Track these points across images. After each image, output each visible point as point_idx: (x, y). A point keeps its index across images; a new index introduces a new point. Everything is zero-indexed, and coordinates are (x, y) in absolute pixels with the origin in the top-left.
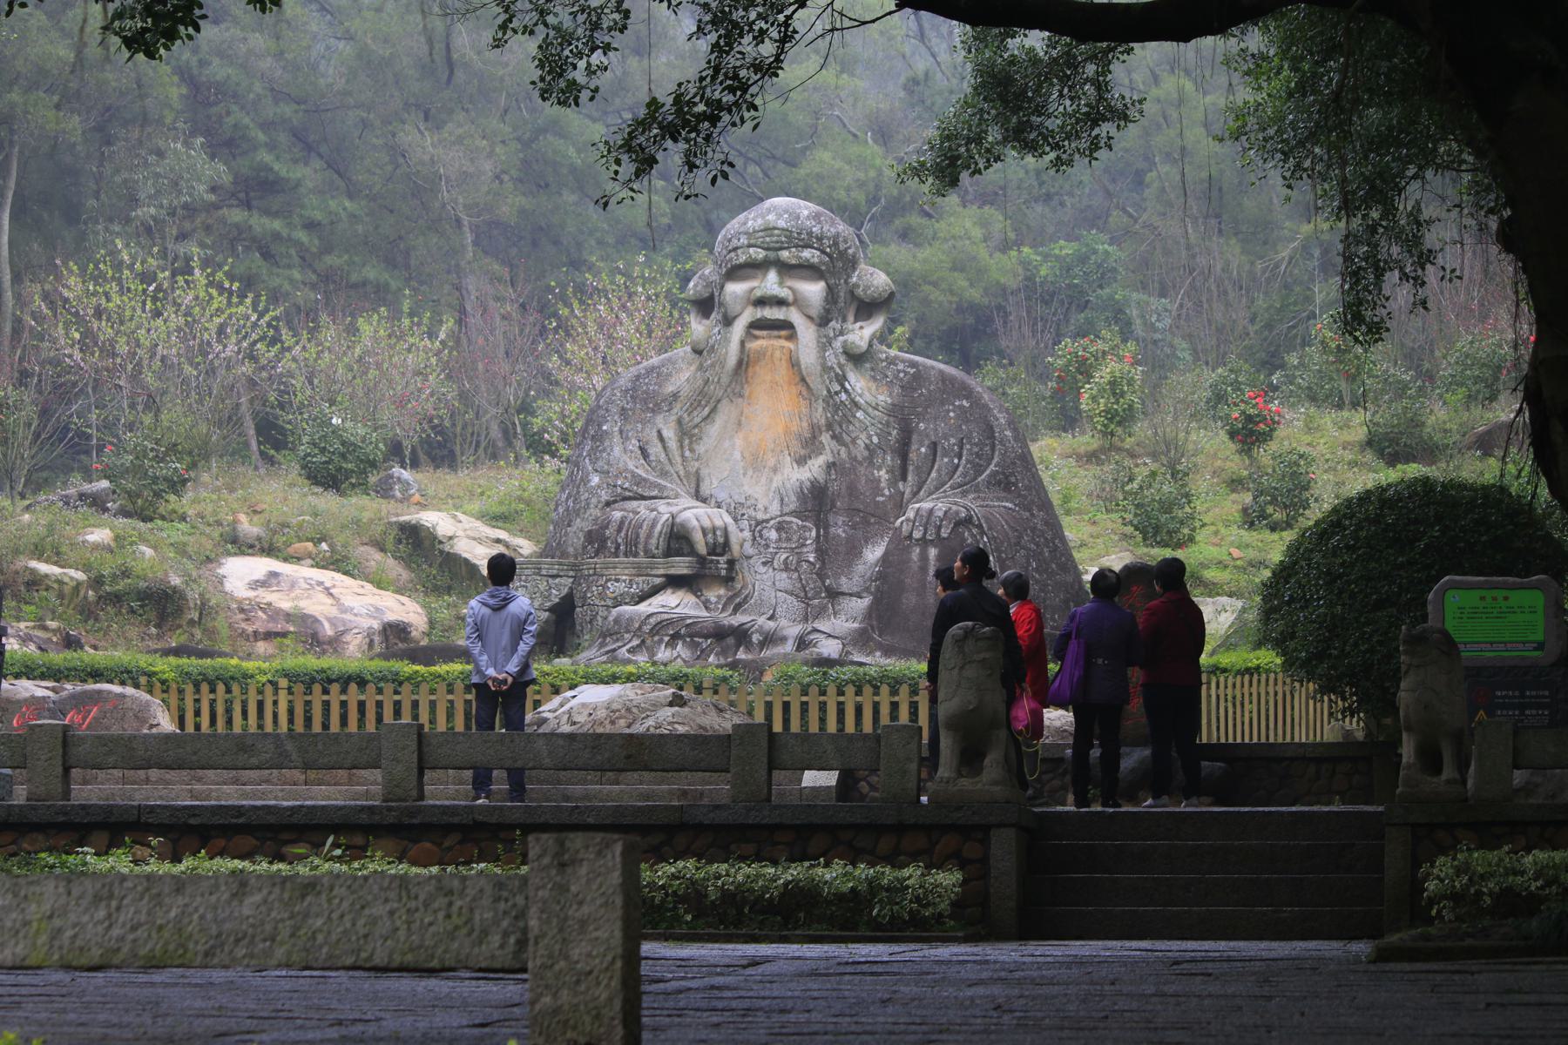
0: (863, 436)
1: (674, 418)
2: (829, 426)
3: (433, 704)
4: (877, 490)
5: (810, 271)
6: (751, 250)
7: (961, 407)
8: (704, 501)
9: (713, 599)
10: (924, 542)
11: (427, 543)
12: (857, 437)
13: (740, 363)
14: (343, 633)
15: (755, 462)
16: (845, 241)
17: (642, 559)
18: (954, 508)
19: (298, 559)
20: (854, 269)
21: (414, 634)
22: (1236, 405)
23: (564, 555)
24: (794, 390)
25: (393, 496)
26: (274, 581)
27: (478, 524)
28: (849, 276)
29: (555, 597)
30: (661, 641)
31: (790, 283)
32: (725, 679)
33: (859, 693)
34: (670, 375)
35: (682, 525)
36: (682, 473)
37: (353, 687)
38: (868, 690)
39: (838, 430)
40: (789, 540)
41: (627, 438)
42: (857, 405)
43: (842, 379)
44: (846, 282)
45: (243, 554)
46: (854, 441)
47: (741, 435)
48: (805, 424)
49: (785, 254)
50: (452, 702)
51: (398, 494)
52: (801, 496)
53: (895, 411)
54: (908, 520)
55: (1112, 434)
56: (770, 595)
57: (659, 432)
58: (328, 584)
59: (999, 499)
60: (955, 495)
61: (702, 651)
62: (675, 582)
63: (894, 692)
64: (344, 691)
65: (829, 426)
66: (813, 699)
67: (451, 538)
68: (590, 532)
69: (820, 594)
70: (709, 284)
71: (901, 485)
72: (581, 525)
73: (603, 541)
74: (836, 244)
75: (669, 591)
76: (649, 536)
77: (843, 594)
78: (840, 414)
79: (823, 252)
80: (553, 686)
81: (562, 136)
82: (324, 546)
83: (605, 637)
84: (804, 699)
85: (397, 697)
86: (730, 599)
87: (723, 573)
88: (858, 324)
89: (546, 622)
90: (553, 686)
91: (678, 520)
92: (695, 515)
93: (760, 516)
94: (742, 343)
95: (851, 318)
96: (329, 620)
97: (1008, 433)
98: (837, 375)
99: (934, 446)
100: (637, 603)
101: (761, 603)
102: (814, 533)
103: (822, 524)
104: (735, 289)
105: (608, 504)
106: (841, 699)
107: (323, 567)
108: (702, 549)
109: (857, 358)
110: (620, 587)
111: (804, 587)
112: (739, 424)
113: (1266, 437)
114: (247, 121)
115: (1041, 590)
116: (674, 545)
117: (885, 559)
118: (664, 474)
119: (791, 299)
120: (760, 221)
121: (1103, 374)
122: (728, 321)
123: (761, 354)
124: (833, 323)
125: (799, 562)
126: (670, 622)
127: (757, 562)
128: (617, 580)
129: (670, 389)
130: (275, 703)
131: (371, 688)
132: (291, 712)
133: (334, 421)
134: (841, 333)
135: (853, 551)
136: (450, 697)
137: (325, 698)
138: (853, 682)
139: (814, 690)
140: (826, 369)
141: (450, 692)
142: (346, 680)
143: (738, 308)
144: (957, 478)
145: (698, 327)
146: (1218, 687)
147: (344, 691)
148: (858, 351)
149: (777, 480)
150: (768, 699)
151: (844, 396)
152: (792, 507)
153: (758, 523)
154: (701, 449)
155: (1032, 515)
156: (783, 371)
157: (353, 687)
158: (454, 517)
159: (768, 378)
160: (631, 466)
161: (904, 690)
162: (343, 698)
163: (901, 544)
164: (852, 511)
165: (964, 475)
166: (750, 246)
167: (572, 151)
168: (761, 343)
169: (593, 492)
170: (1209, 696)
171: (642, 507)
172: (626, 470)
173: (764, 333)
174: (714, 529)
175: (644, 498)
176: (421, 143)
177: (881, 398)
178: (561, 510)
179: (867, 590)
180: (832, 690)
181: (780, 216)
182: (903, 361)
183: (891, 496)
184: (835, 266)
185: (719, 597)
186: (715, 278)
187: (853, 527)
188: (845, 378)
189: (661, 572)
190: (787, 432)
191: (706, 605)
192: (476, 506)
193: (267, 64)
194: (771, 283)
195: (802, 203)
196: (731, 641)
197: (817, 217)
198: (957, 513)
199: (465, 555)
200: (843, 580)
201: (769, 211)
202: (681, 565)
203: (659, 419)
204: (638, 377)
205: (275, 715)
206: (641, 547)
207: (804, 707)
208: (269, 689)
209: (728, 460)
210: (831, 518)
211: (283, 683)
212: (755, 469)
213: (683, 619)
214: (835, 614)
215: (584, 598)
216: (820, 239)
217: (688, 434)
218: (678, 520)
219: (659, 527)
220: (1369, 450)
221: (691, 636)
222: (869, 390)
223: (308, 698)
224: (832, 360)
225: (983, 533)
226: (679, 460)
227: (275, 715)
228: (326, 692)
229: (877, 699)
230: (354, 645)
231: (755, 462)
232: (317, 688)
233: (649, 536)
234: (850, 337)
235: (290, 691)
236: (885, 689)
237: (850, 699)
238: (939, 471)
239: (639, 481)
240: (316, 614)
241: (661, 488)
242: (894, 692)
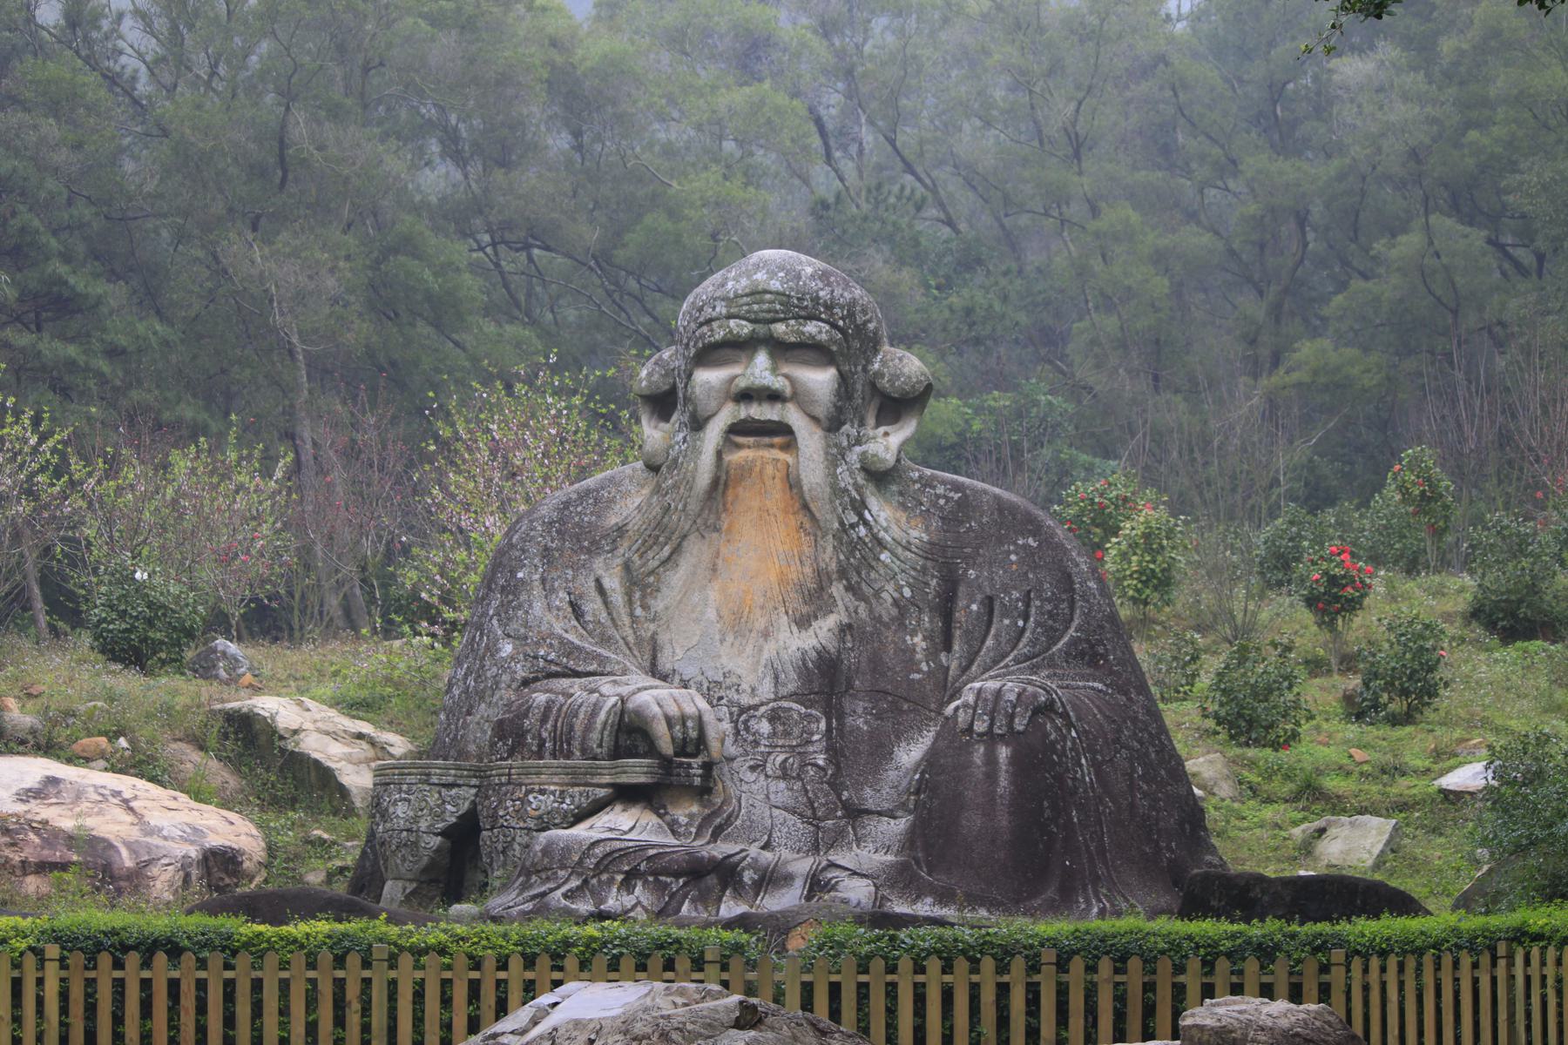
0: (890, 587)
1: (619, 561)
2: (843, 573)
3: (284, 985)
4: (912, 665)
6: (732, 323)
7: (1026, 547)
8: (664, 678)
9: (683, 820)
10: (990, 738)
11: (263, 739)
12: (882, 589)
13: (715, 483)
14: (148, 863)
15: (737, 624)
16: (864, 312)
17: (577, 761)
18: (1030, 688)
19: (85, 760)
20: (876, 351)
21: (246, 864)
22: (1313, 563)
23: (462, 754)
24: (793, 521)
25: (217, 677)
26: (52, 790)
27: (332, 713)
28: (869, 362)
29: (451, 815)
30: (611, 881)
31: (786, 369)
32: (738, 948)
33: (947, 968)
34: (612, 501)
35: (638, 713)
36: (631, 639)
37: (161, 958)
38: (961, 965)
39: (855, 579)
40: (787, 734)
41: (553, 590)
42: (881, 543)
43: (859, 507)
44: (865, 370)
45: (11, 752)
46: (877, 594)
47: (716, 585)
48: (808, 570)
49: (780, 328)
50: (313, 982)
51: (223, 673)
52: (803, 670)
53: (932, 551)
54: (966, 706)
55: (1146, 603)
56: (762, 811)
57: (598, 581)
58: (127, 795)
59: (1083, 678)
60: (1021, 671)
61: (672, 896)
62: (626, 795)
63: (1002, 968)
64: (146, 964)
65: (843, 573)
66: (876, 979)
67: (295, 732)
68: (501, 722)
69: (835, 814)
70: (669, 373)
71: (943, 657)
72: (487, 712)
73: (520, 735)
74: (851, 315)
75: (618, 808)
76: (588, 728)
77: (869, 812)
78: (857, 557)
79: (834, 326)
80: (471, 957)
81: (419, 258)
82: (123, 742)
83: (528, 874)
84: (863, 978)
85: (229, 974)
86: (707, 820)
87: (697, 781)
88: (882, 429)
89: (438, 850)
90: (471, 957)
91: (630, 705)
92: (653, 698)
93: (746, 700)
94: (719, 454)
95: (871, 421)
96: (128, 845)
97: (1091, 584)
98: (853, 500)
99: (989, 603)
100: (572, 825)
101: (751, 825)
102: (823, 726)
103: (833, 711)
104: (709, 378)
105: (526, 682)
106: (920, 978)
107: (121, 772)
108: (666, 747)
109: (880, 477)
110: (548, 802)
111: (811, 803)
112: (714, 569)
113: (1353, 605)
114: (36, 223)
115: (1152, 808)
116: (625, 741)
117: (931, 760)
118: (605, 640)
119: (788, 391)
120: (744, 282)
121: (1130, 528)
122: (698, 424)
123: (746, 470)
124: (846, 427)
125: (803, 766)
126: (624, 854)
127: (742, 766)
128: (542, 792)
129: (613, 520)
130: (40, 982)
131: (188, 959)
132: (64, 996)
133: (138, 575)
134: (858, 442)
135: (881, 751)
136: (311, 974)
137: (118, 974)
138: (938, 952)
139: (878, 965)
141: (312, 965)
142: (149, 947)
143: (713, 404)
144: (1023, 647)
145: (653, 433)
146: (1527, 962)
147: (146, 964)
148: (882, 467)
149: (769, 650)
150: (807, 978)
151: (862, 531)
152: (791, 687)
153: (743, 710)
154: (658, 605)
155: (1130, 699)
156: (776, 495)
157: (161, 958)
158: (300, 704)
159: (756, 504)
160: (558, 630)
161: (1018, 964)
162: (146, 974)
163: (955, 740)
164: (876, 694)
165: (1033, 643)
166: (730, 317)
167: (427, 274)
168: (746, 453)
169: (503, 666)
170: (1511, 978)
171: (576, 687)
172: (551, 635)
173: (751, 440)
174: (684, 719)
175: (578, 674)
176: (250, 257)
177: (914, 533)
178: (456, 692)
179: (903, 806)
180: (905, 964)
181: (772, 275)
182: (943, 482)
183: (929, 672)
184: (849, 346)
185: (691, 816)
186: (679, 363)
187: (878, 717)
188: (864, 505)
189: (607, 779)
190: (782, 581)
191: (673, 828)
192: (328, 689)
193: (61, 157)
195: (803, 257)
196: (712, 880)
197: (824, 276)
198: (1035, 696)
199: (315, 755)
200: (868, 791)
201: (757, 267)
202: (637, 771)
203: (598, 564)
204: (567, 504)
205: (40, 1002)
206: (576, 743)
207: (863, 991)
208: (30, 961)
209: (697, 621)
210: (847, 704)
211: (53, 951)
212: (737, 634)
213: (643, 848)
214: (858, 841)
215: (495, 817)
216: (829, 307)
217: (639, 584)
218: (630, 705)
219: (602, 716)
220: (1474, 624)
221: (656, 873)
222: (898, 521)
223: (92, 974)
224: (845, 480)
225: (1070, 725)
226: (626, 620)
227: (40, 1002)
228: (118, 964)
229: (975, 978)
230: (162, 881)
231: (737, 624)
232: (105, 960)
233: (588, 728)
234: (872, 448)
235: (63, 963)
236: (988, 964)
237: (934, 978)
238: (997, 636)
239: (571, 650)
240: (111, 837)
241: (602, 660)
242: (1002, 968)
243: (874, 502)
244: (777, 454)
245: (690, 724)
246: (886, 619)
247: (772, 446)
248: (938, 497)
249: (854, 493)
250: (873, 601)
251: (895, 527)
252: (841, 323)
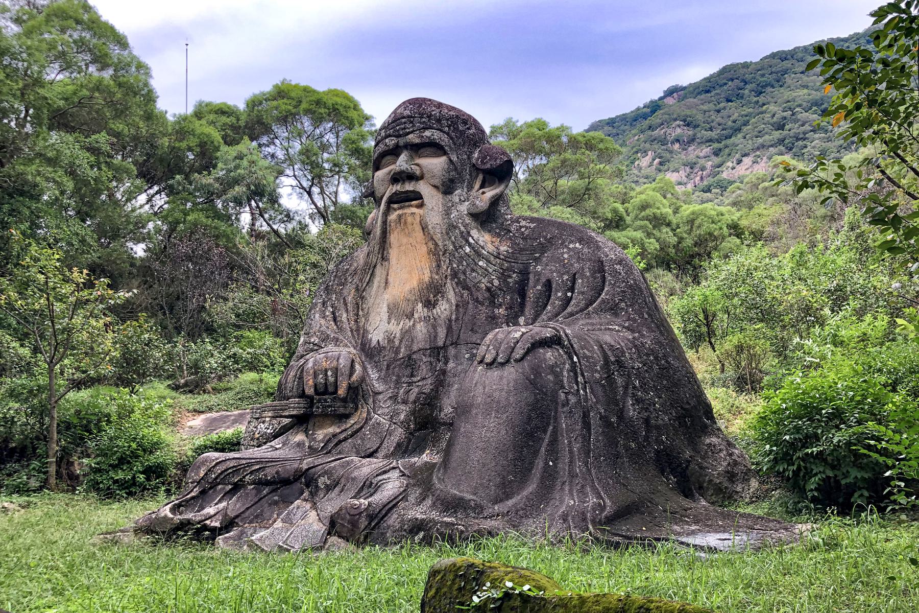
5: (436, 148)
39: (462, 277)
42: (479, 254)
43: (466, 236)
98: (462, 233)
119: (418, 173)
213: (250, 465)
216: (439, 121)
243: (474, 233)
244: (414, 210)
245: (329, 373)
246: (480, 299)
248: (521, 227)
249: (462, 228)
250: (473, 290)
251: (489, 245)
252: (446, 129)
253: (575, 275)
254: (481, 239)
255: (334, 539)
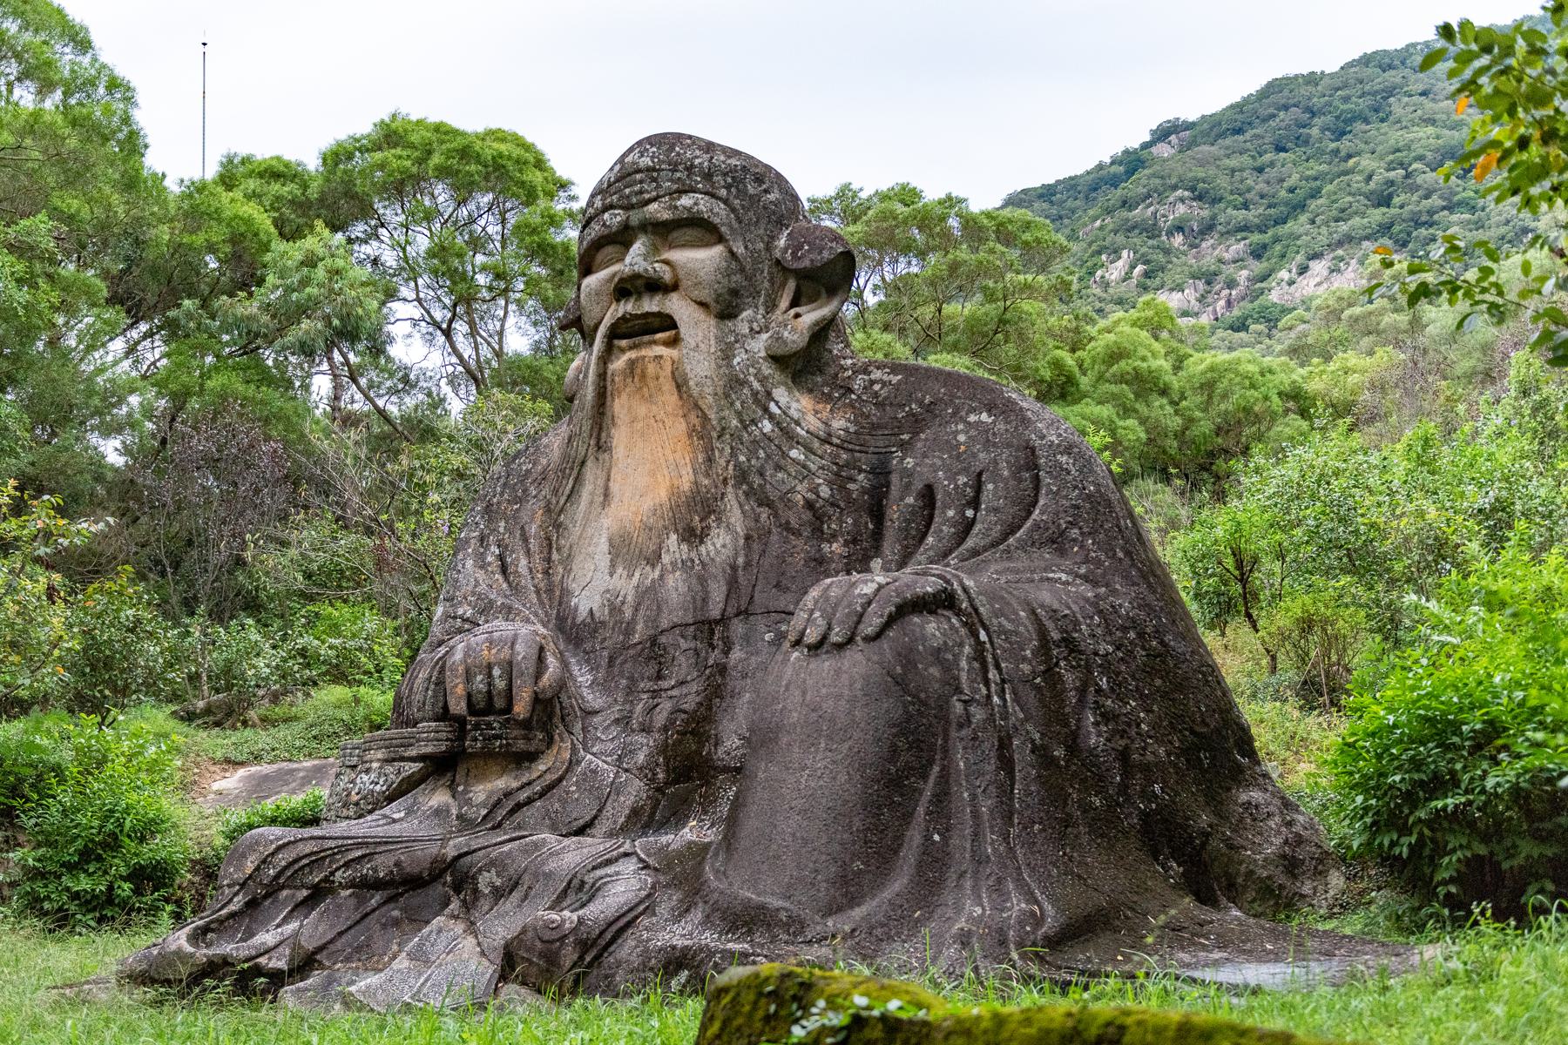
5: (702, 229)
39: (757, 481)
43: (763, 400)
98: (755, 394)
119: (667, 277)
140: (735, 383)
194: (636, 258)
213: (343, 850)
216: (708, 176)
243: (780, 394)
245: (496, 672)
246: (794, 523)
247: (655, 342)
248: (872, 382)
249: (756, 385)
250: (780, 506)
252: (723, 192)
253: (980, 474)
254: (794, 405)
255: (511, 990)
